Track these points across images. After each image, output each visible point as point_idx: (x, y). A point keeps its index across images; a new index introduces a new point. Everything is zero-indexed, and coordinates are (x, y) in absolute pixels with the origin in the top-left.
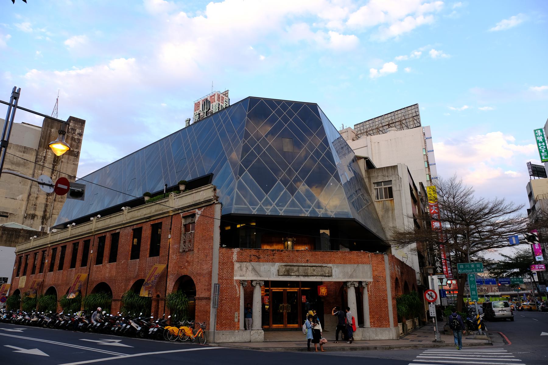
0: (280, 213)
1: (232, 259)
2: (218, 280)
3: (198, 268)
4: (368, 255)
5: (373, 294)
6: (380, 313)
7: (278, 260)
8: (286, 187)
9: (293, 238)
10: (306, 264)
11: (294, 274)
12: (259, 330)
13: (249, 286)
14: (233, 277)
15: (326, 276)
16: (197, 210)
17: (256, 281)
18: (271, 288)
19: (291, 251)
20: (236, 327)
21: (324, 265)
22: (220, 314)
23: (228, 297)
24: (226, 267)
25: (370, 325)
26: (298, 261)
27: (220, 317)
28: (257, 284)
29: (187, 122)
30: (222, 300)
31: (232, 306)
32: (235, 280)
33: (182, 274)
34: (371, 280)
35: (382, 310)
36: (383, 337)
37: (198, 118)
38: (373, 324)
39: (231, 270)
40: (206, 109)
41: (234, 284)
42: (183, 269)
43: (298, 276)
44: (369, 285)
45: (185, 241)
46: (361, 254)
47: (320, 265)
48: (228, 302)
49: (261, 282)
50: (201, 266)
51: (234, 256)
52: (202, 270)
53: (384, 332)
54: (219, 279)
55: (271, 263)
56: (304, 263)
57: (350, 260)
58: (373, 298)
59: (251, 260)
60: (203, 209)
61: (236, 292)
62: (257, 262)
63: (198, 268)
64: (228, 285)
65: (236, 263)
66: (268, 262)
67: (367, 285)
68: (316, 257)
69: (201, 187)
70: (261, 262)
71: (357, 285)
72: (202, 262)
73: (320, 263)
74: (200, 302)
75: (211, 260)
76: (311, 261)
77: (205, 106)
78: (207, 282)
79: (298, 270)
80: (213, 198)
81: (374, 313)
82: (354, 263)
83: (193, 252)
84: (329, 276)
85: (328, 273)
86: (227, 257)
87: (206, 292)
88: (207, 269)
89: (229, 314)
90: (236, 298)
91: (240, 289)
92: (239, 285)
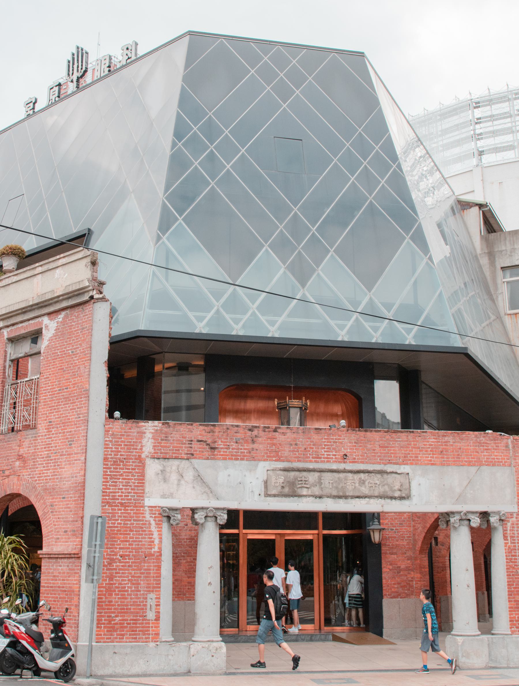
0: (269, 331)
1: (141, 449)
2: (103, 506)
3: (47, 473)
4: (505, 441)
7: (267, 453)
8: (284, 265)
9: (302, 400)
10: (342, 466)
11: (310, 493)
12: (213, 641)
13: (187, 525)
14: (143, 500)
15: (395, 498)
16: (46, 320)
17: (205, 511)
18: (245, 531)
19: (300, 432)
20: (149, 634)
21: (389, 468)
22: (106, 598)
23: (129, 552)
24: (124, 472)
25: (511, 628)
26: (321, 458)
27: (106, 605)
28: (209, 519)
29: (29, 105)
30: (111, 561)
31: (140, 577)
32: (149, 507)
33: (6, 491)
37: (57, 95)
39: (138, 480)
40: (78, 71)
41: (144, 517)
42: (8, 476)
43: (320, 497)
44: (509, 521)
45: (15, 403)
46: (487, 438)
48: (129, 566)
49: (219, 513)
50: (56, 469)
51: (144, 441)
52: (57, 479)
54: (105, 503)
56: (336, 462)
57: (458, 455)
59: (192, 454)
60: (61, 316)
61: (151, 538)
62: (207, 459)
63: (47, 473)
64: (130, 521)
65: (152, 460)
66: (237, 459)
67: (502, 520)
69: (58, 257)
70: (219, 459)
71: (476, 522)
72: (58, 459)
73: (379, 463)
74: (53, 566)
75: (83, 453)
76: (355, 459)
77: (73, 64)
78: (71, 511)
79: (320, 482)
80: (87, 284)
83: (34, 431)
84: (401, 498)
85: (400, 490)
86: (126, 445)
87: (69, 538)
88: (73, 477)
89: (131, 598)
90: (152, 555)
91: (161, 531)
92: (159, 521)
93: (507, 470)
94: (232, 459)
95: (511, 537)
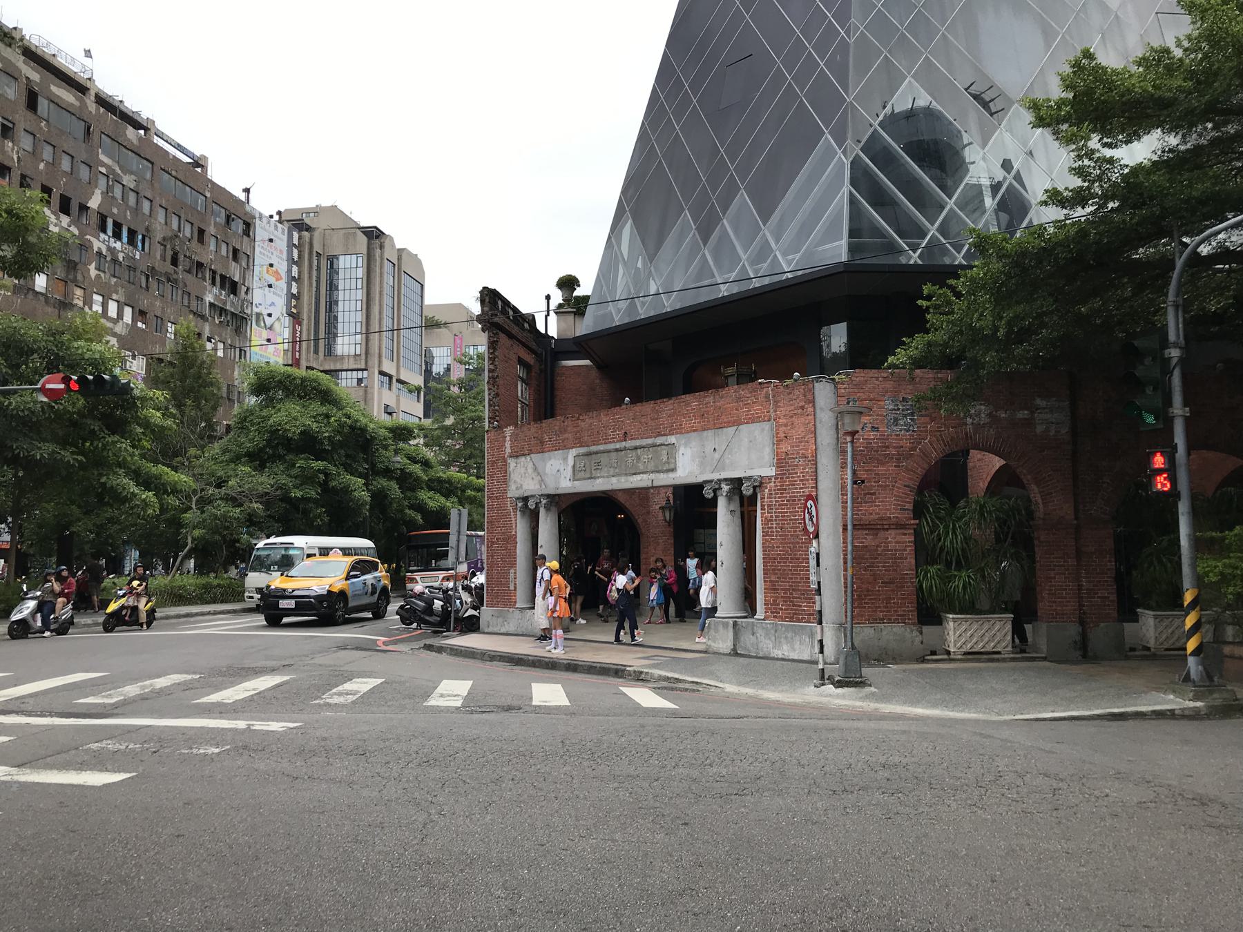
4: (765, 390)
5: (776, 516)
6: (792, 574)
21: (659, 440)
25: (766, 612)
34: (771, 472)
35: (798, 566)
36: (794, 650)
38: (772, 609)
47: (649, 441)
53: (798, 638)
55: (561, 451)
58: (776, 528)
66: (556, 450)
68: (643, 420)
81: (776, 574)
82: (729, 424)
93: (766, 426)
94: (552, 450)
95: (769, 506)
